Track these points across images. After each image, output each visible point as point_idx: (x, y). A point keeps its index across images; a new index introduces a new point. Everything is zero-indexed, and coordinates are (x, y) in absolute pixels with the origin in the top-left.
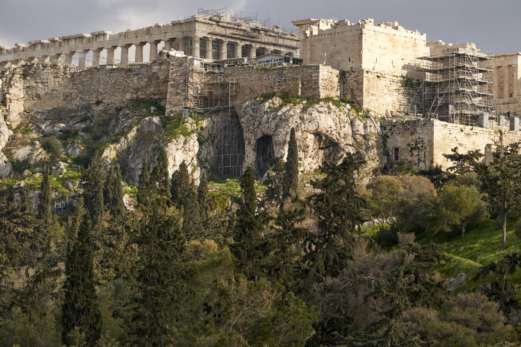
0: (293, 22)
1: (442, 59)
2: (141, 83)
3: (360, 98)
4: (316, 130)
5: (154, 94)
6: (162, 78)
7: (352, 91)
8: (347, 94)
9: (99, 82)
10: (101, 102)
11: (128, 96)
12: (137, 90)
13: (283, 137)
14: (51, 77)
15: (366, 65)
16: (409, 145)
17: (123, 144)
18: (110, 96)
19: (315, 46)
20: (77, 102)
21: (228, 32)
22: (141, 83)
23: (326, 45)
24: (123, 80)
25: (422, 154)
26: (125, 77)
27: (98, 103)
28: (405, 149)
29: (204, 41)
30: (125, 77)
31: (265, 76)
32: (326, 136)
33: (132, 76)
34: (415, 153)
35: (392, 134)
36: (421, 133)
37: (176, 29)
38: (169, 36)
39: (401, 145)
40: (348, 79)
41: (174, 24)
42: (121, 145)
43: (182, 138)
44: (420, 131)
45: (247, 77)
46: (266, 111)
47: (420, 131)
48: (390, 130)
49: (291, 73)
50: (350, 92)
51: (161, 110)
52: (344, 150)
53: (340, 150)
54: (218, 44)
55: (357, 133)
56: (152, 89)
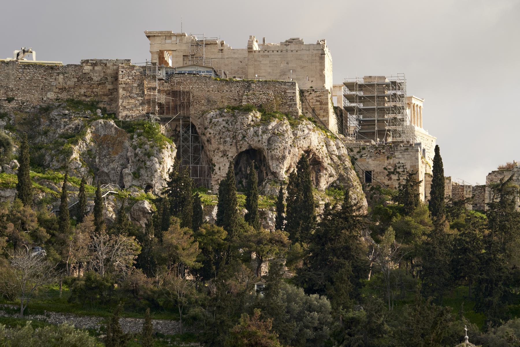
0: (146, 33)
1: (361, 87)
2: (69, 83)
3: (325, 119)
4: (309, 147)
5: (86, 96)
6: (97, 80)
7: (313, 110)
8: (307, 113)
10: (13, 99)
12: (63, 89)
13: (282, 152)
16: (385, 168)
17: (82, 146)
18: (25, 93)
19: (261, 61)
22: (69, 83)
23: (276, 62)
24: (42, 77)
26: (45, 75)
28: (380, 173)
30: (45, 75)
31: (226, 88)
32: (314, 154)
33: (55, 74)
34: (394, 177)
35: (361, 156)
39: (375, 169)
40: (307, 98)
42: (80, 147)
44: (400, 156)
45: (203, 87)
46: (250, 124)
47: (400, 156)
48: (359, 152)
49: (259, 87)
50: (311, 111)
52: (326, 169)
53: (321, 169)
55: (333, 153)
56: (82, 91)
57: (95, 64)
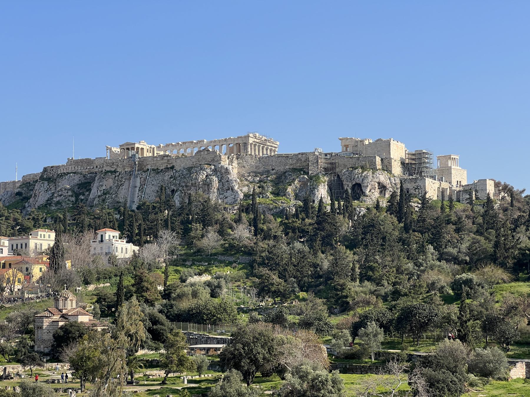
9: (272, 161)
11: (287, 167)
12: (292, 164)
14: (249, 159)
15: (392, 157)
20: (262, 169)
21: (258, 141)
25: (420, 191)
27: (273, 170)
29: (251, 144)
31: (351, 160)
36: (419, 183)
37: (240, 139)
38: (236, 142)
41: (238, 138)
43: (323, 184)
51: (307, 174)
54: (255, 145)
57: (303, 154)
